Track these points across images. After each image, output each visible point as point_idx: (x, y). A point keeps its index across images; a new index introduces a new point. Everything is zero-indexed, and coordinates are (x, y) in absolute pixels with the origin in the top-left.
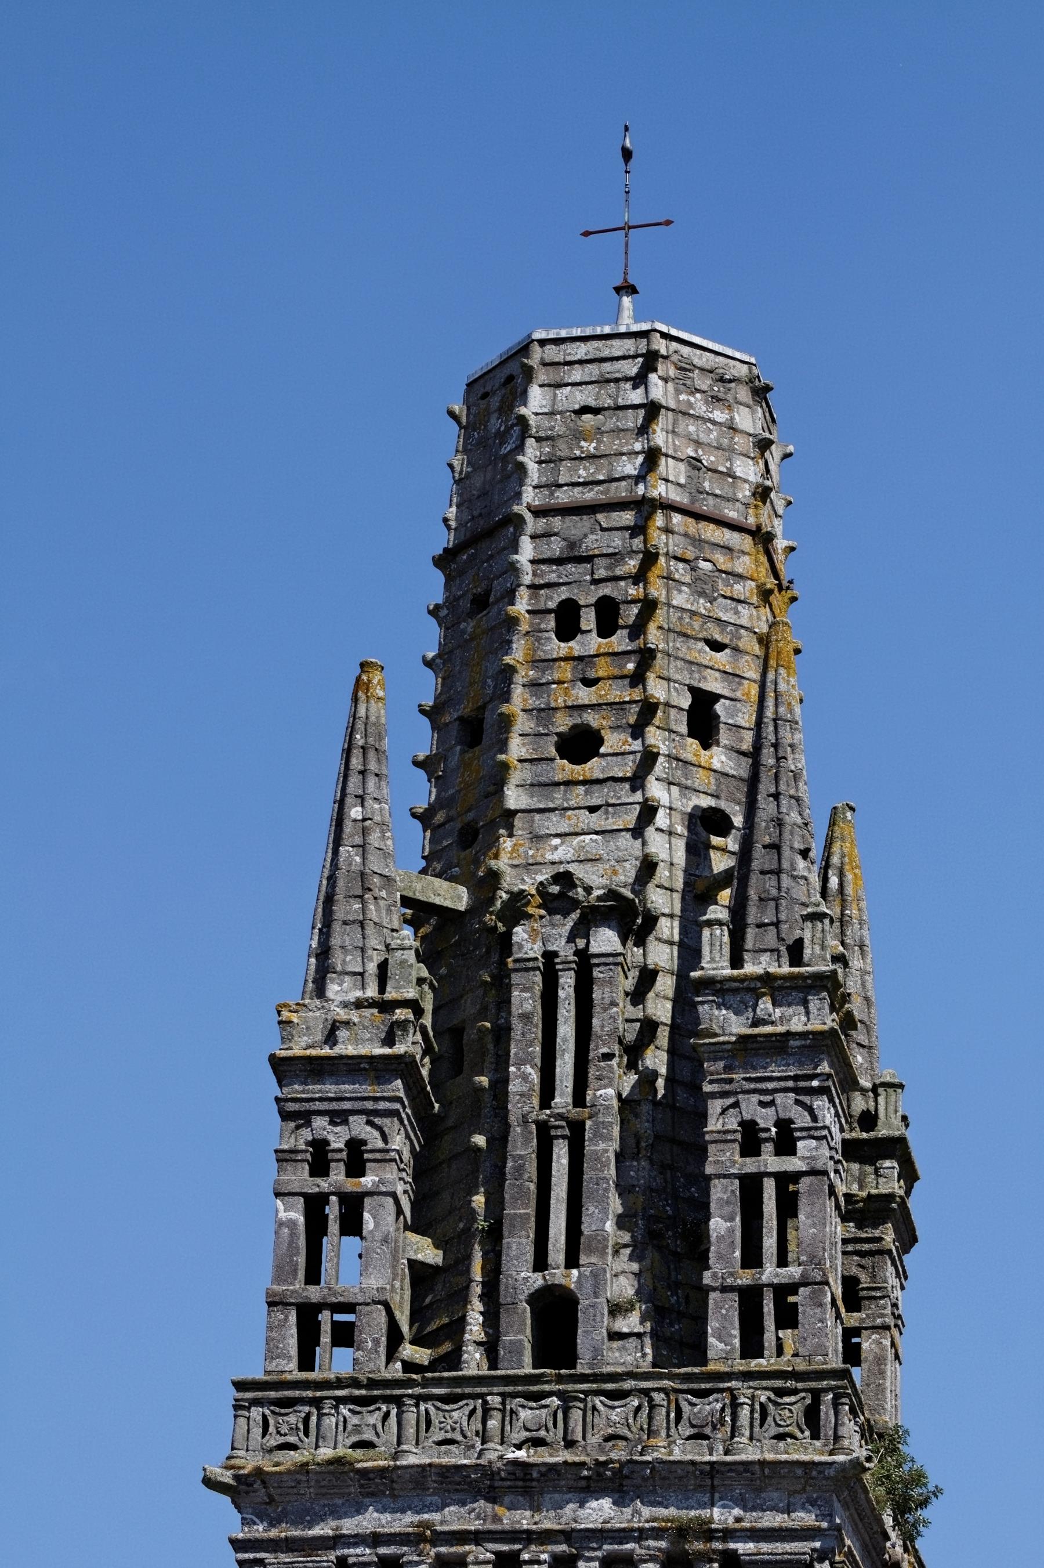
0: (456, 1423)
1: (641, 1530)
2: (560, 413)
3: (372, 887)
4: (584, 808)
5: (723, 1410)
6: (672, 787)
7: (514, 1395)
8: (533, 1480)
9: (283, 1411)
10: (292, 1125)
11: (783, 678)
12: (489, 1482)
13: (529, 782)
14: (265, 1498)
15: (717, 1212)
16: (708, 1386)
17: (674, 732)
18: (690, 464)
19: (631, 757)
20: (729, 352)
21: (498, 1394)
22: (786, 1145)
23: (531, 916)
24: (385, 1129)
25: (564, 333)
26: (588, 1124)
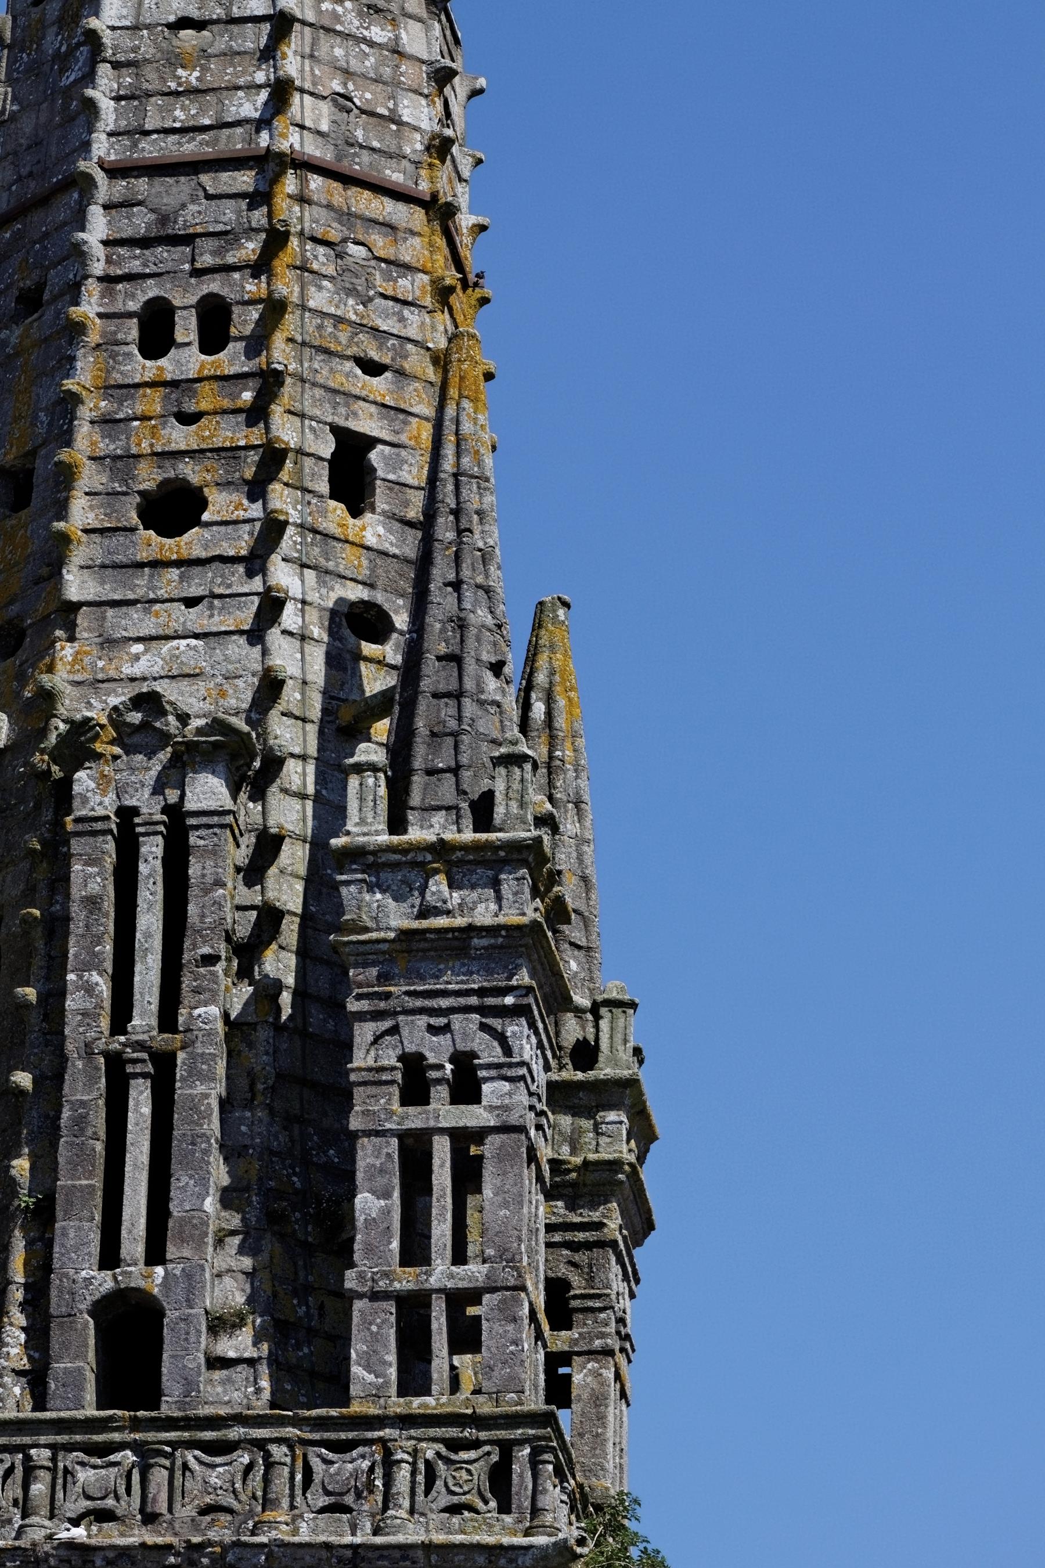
2: (148, 27)
5: (371, 1470)
6: (306, 571)
7: (70, 1448)
11: (468, 415)
13: (98, 562)
16: (351, 1435)
17: (310, 492)
19: (247, 527)
21: (46, 1446)
23: (99, 756)
26: (181, 1056)
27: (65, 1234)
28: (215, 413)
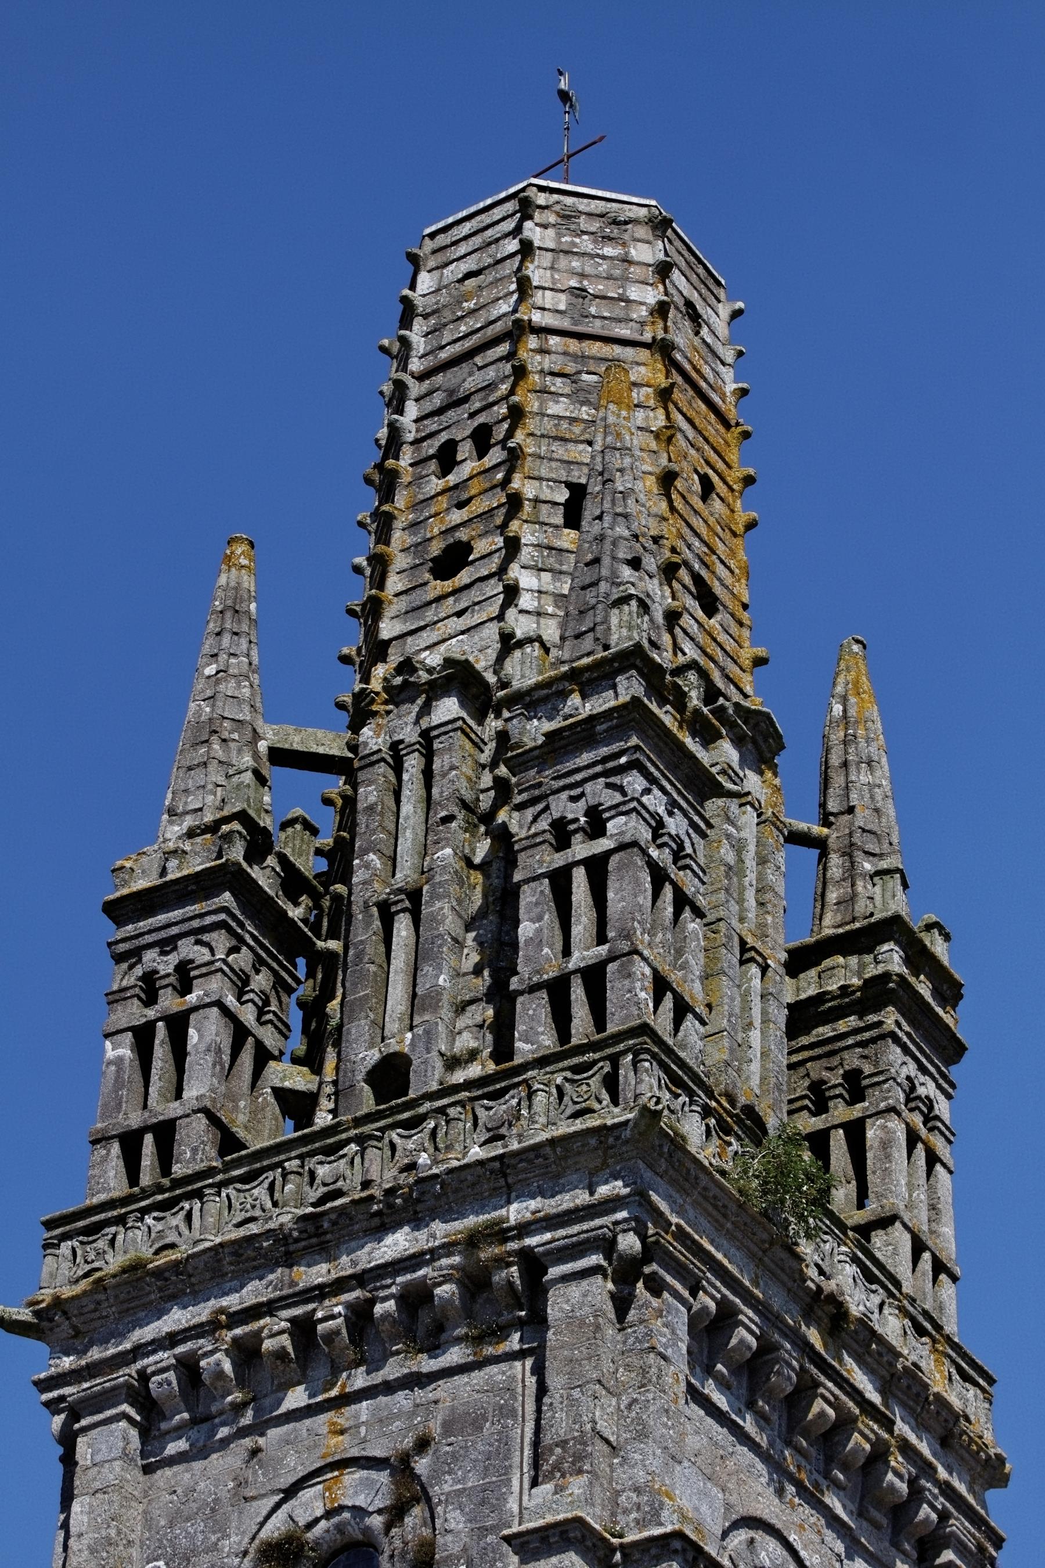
0: (256, 1200)
1: (432, 1251)
2: (445, 287)
3: (218, 729)
4: (453, 615)
5: (519, 1104)
6: (543, 574)
7: (312, 1154)
8: (325, 1233)
9: (91, 1239)
10: (125, 966)
11: (613, 412)
12: (283, 1249)
14: (70, 1331)
15: (526, 917)
16: (503, 1084)
17: (546, 524)
18: (572, 294)
19: (497, 555)
20: (625, 198)
21: (296, 1158)
23: (375, 714)
24: (213, 944)
25: (450, 220)
26: (426, 888)
27: (348, 1034)
28: (480, 494)
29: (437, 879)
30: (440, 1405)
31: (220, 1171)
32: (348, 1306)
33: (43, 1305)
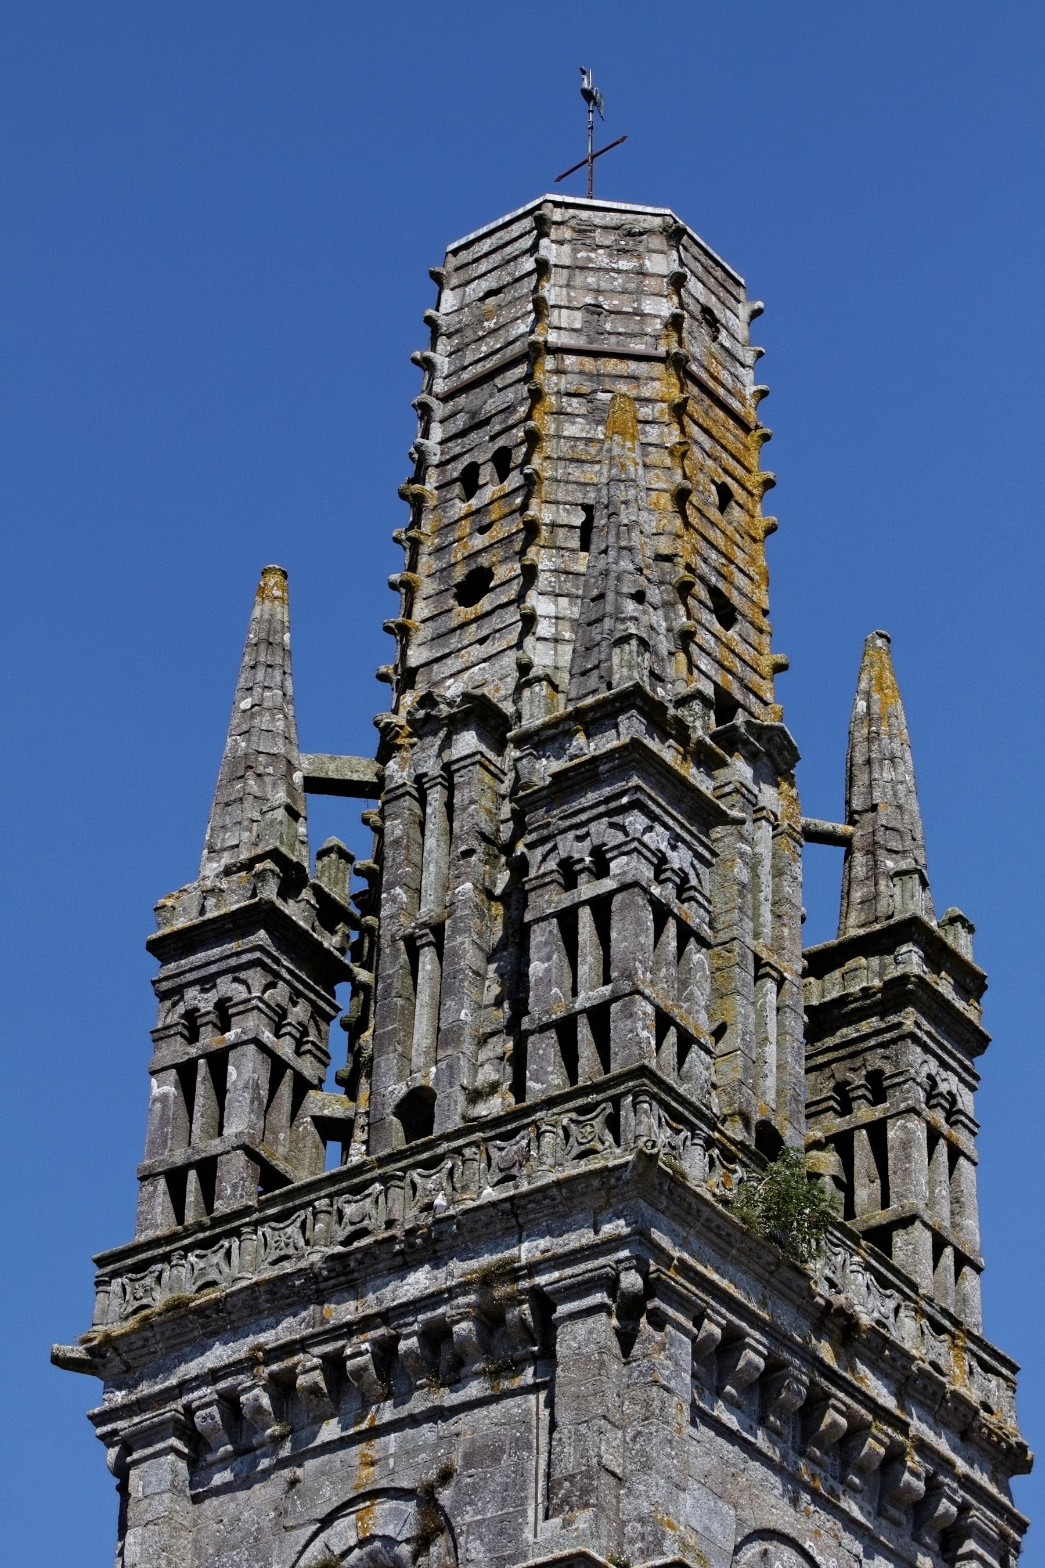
0: (289, 1238)
1: (449, 1290)
2: (467, 306)
3: (253, 765)
4: (475, 643)
5: (528, 1145)
6: (560, 599)
7: (340, 1193)
8: (353, 1271)
9: (139, 1276)
11: (618, 444)
12: (314, 1287)
13: (429, 638)
14: (122, 1366)
16: (514, 1125)
17: (563, 549)
18: (588, 311)
19: (516, 581)
22: (601, 869)
23: (400, 747)
24: (250, 981)
25: (472, 236)
26: (448, 922)
27: (379, 1067)
28: (501, 519)
29: (459, 913)
30: (462, 1438)
31: (256, 1210)
32: (374, 1342)
33: (95, 1343)
